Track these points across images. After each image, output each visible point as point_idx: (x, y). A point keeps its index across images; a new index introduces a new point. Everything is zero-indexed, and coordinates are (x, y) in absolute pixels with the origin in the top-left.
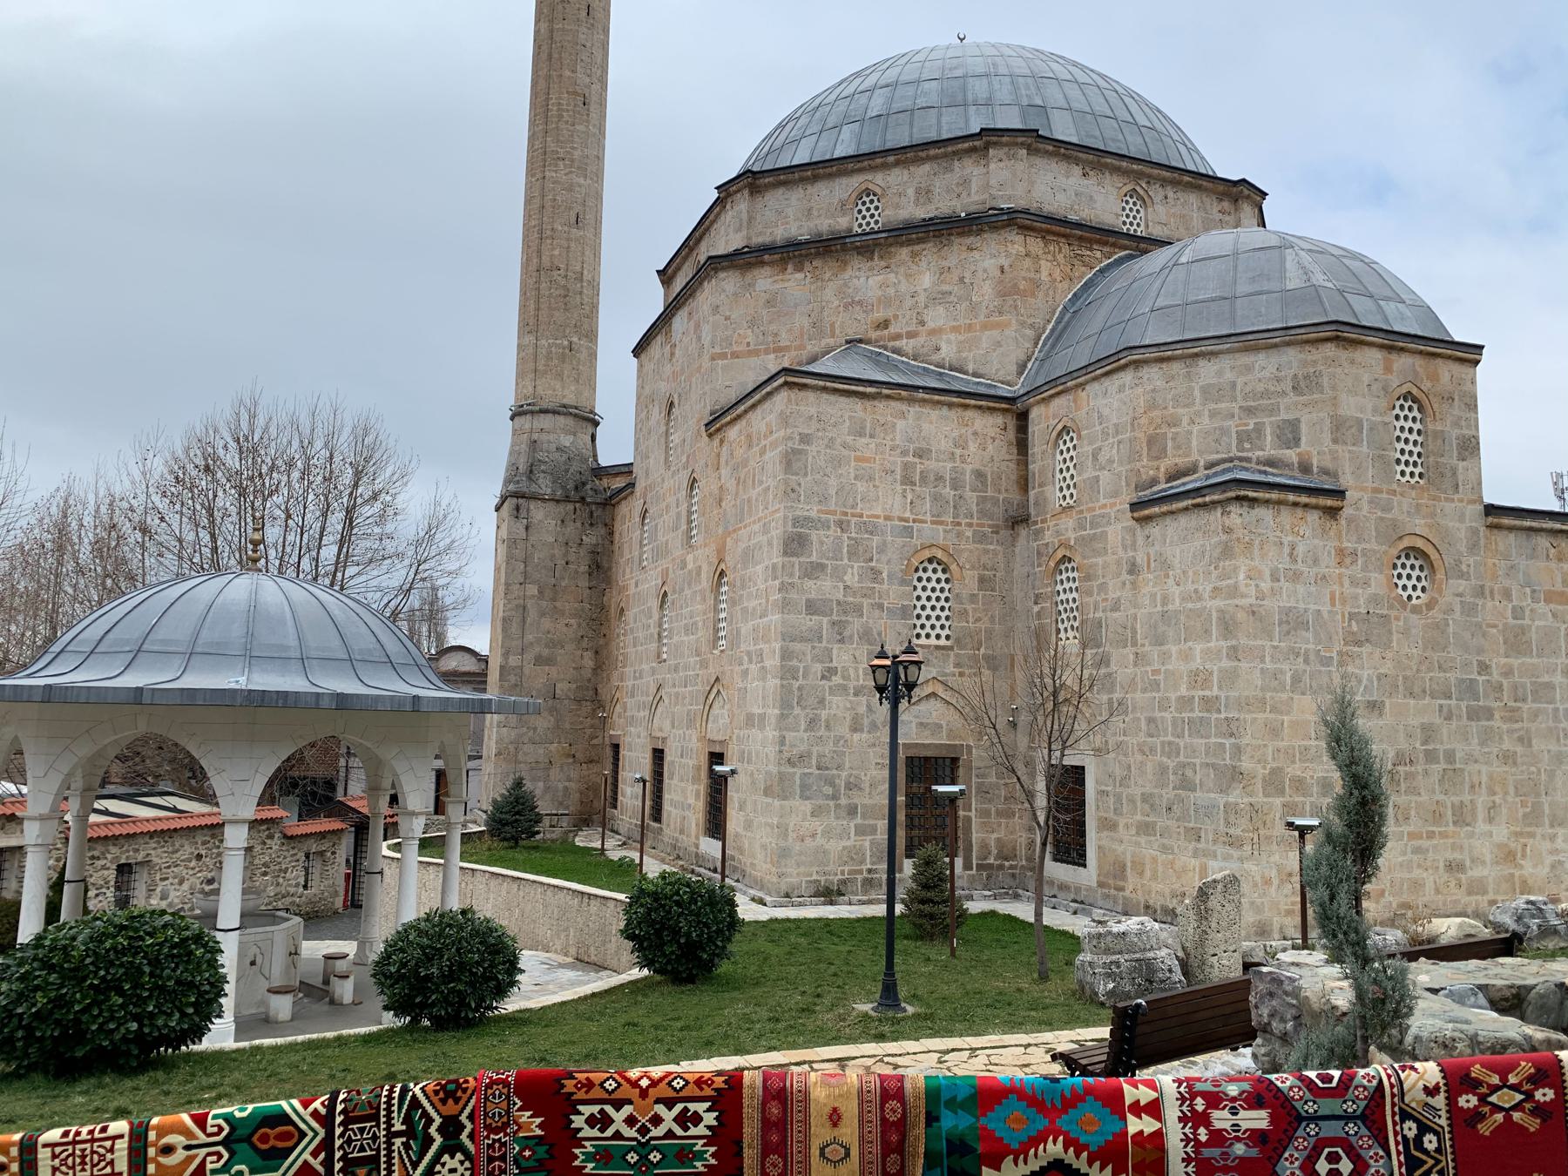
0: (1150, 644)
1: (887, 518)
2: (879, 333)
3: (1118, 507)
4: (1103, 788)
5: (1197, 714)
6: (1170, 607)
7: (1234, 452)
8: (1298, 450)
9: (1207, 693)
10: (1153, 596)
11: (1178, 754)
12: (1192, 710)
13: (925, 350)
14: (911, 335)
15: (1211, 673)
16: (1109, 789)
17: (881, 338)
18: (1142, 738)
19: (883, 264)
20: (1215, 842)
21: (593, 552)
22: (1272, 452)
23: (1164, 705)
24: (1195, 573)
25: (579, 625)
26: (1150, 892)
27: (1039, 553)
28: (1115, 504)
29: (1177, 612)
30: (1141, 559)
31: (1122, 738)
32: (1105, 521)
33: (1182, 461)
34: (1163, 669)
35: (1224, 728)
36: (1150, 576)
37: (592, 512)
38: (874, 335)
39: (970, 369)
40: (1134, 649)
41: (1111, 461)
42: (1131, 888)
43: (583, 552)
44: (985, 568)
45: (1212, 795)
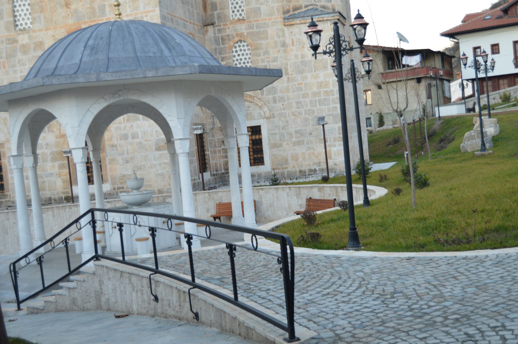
1: (181, 19)
3: (273, 20)
4: (273, 132)
5: (323, 97)
6: (306, 59)
7: (313, 2)
8: (331, 4)
10: (296, 56)
11: (314, 113)
12: (320, 96)
15: (329, 82)
16: (276, 132)
20: (334, 141)
22: (324, 4)
23: (305, 96)
26: (302, 166)
27: (223, 39)
28: (271, 19)
30: (288, 41)
31: (283, 111)
33: (297, 4)
34: (303, 82)
36: (294, 48)
40: (287, 76)
42: (291, 166)
45: (332, 125)
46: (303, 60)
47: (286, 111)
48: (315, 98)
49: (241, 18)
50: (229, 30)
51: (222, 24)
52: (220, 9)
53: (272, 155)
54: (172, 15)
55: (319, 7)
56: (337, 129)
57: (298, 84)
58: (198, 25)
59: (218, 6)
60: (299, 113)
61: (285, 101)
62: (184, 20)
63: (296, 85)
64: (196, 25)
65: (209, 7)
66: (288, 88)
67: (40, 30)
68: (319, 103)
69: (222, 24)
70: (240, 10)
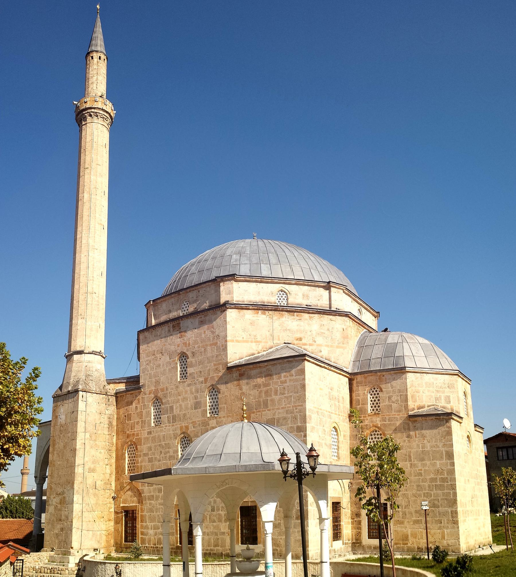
0: (417, 461)
2: (298, 342)
5: (438, 483)
6: (426, 449)
9: (442, 476)
10: (418, 446)
11: (431, 496)
12: (437, 482)
13: (316, 351)
14: (310, 345)
17: (299, 344)
18: (414, 492)
19: (298, 318)
23: (424, 481)
24: (436, 439)
29: (428, 452)
32: (395, 420)
33: (422, 404)
35: (450, 487)
38: (296, 342)
39: (333, 360)
41: (397, 401)
44: (345, 432)
45: (446, 509)
46: (424, 450)
47: (408, 492)
48: (433, 484)
49: (377, 412)
50: (368, 421)
51: (362, 416)
52: (362, 404)
53: (395, 531)
54: (318, 409)
55: (439, 407)
56: (450, 512)
57: (419, 470)
58: (343, 416)
59: (360, 401)
60: (419, 495)
61: (407, 484)
62: (329, 412)
63: (418, 470)
64: (341, 416)
65: (354, 402)
66: (410, 472)
67: (224, 417)
68: (436, 488)
69: (362, 416)
70: (377, 406)
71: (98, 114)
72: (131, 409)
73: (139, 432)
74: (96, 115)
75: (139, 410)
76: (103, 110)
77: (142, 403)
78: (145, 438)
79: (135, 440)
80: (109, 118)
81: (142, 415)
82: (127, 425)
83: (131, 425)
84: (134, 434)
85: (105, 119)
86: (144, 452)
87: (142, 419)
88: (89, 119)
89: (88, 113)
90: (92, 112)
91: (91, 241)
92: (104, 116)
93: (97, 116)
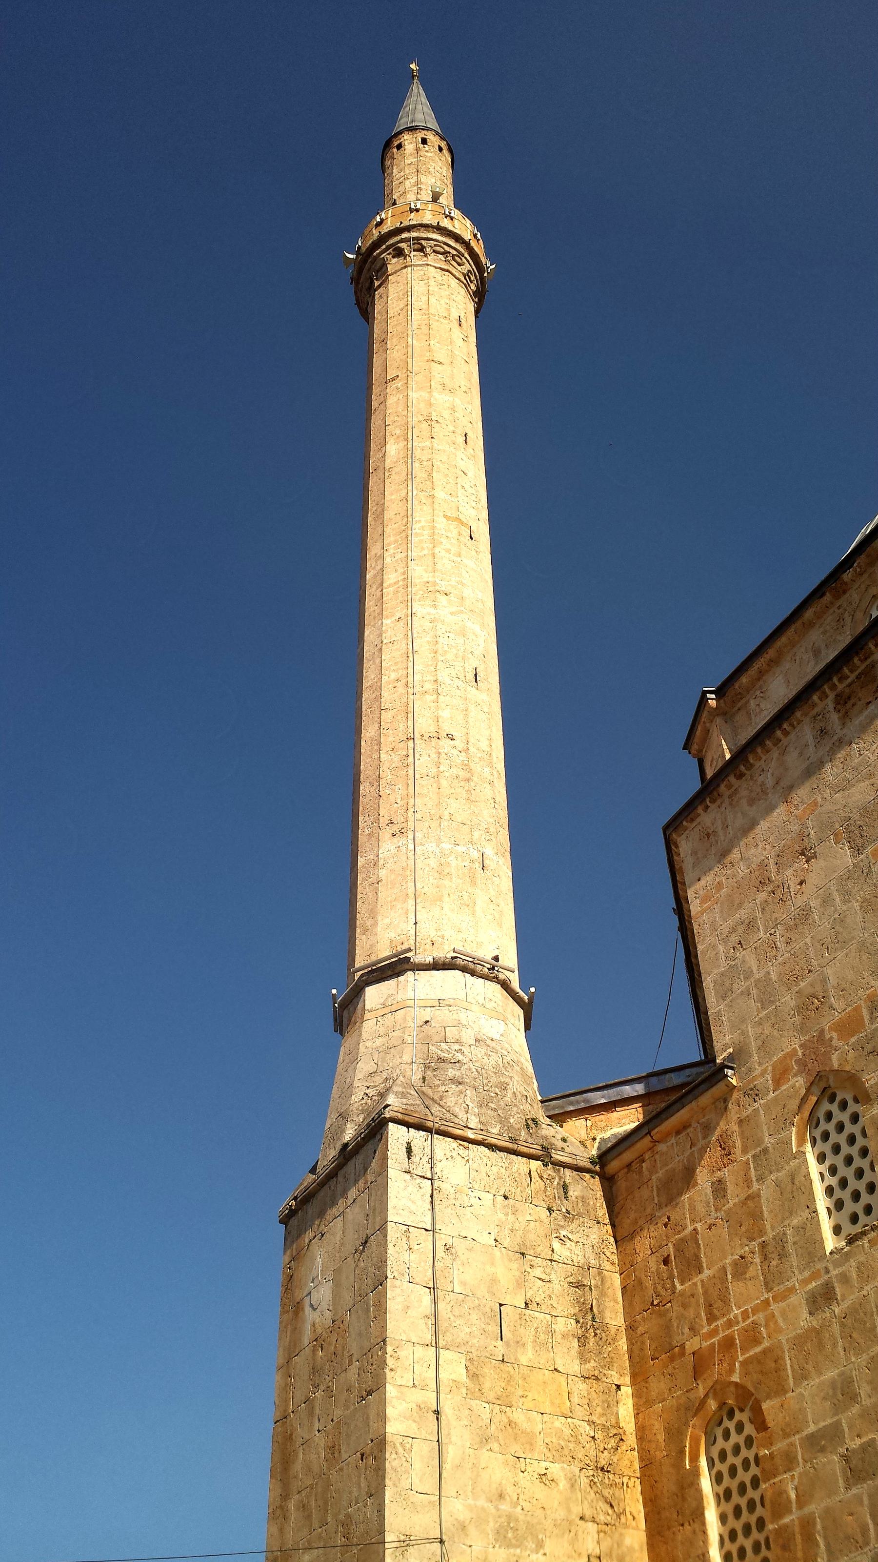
21: (579, 1285)
25: (573, 1483)
37: (565, 1187)
43: (558, 1284)
71: (423, 242)
72: (692, 1209)
73: (760, 1317)
74: (416, 246)
75: (734, 1195)
76: (439, 229)
77: (745, 1151)
78: (799, 1342)
79: (745, 1373)
80: (466, 255)
81: (757, 1216)
82: (684, 1306)
83: (705, 1293)
84: (728, 1344)
85: (454, 259)
86: (812, 1428)
87: (762, 1232)
88: (393, 264)
89: (388, 248)
90: (402, 241)
91: (420, 573)
92: (447, 249)
93: (422, 249)
